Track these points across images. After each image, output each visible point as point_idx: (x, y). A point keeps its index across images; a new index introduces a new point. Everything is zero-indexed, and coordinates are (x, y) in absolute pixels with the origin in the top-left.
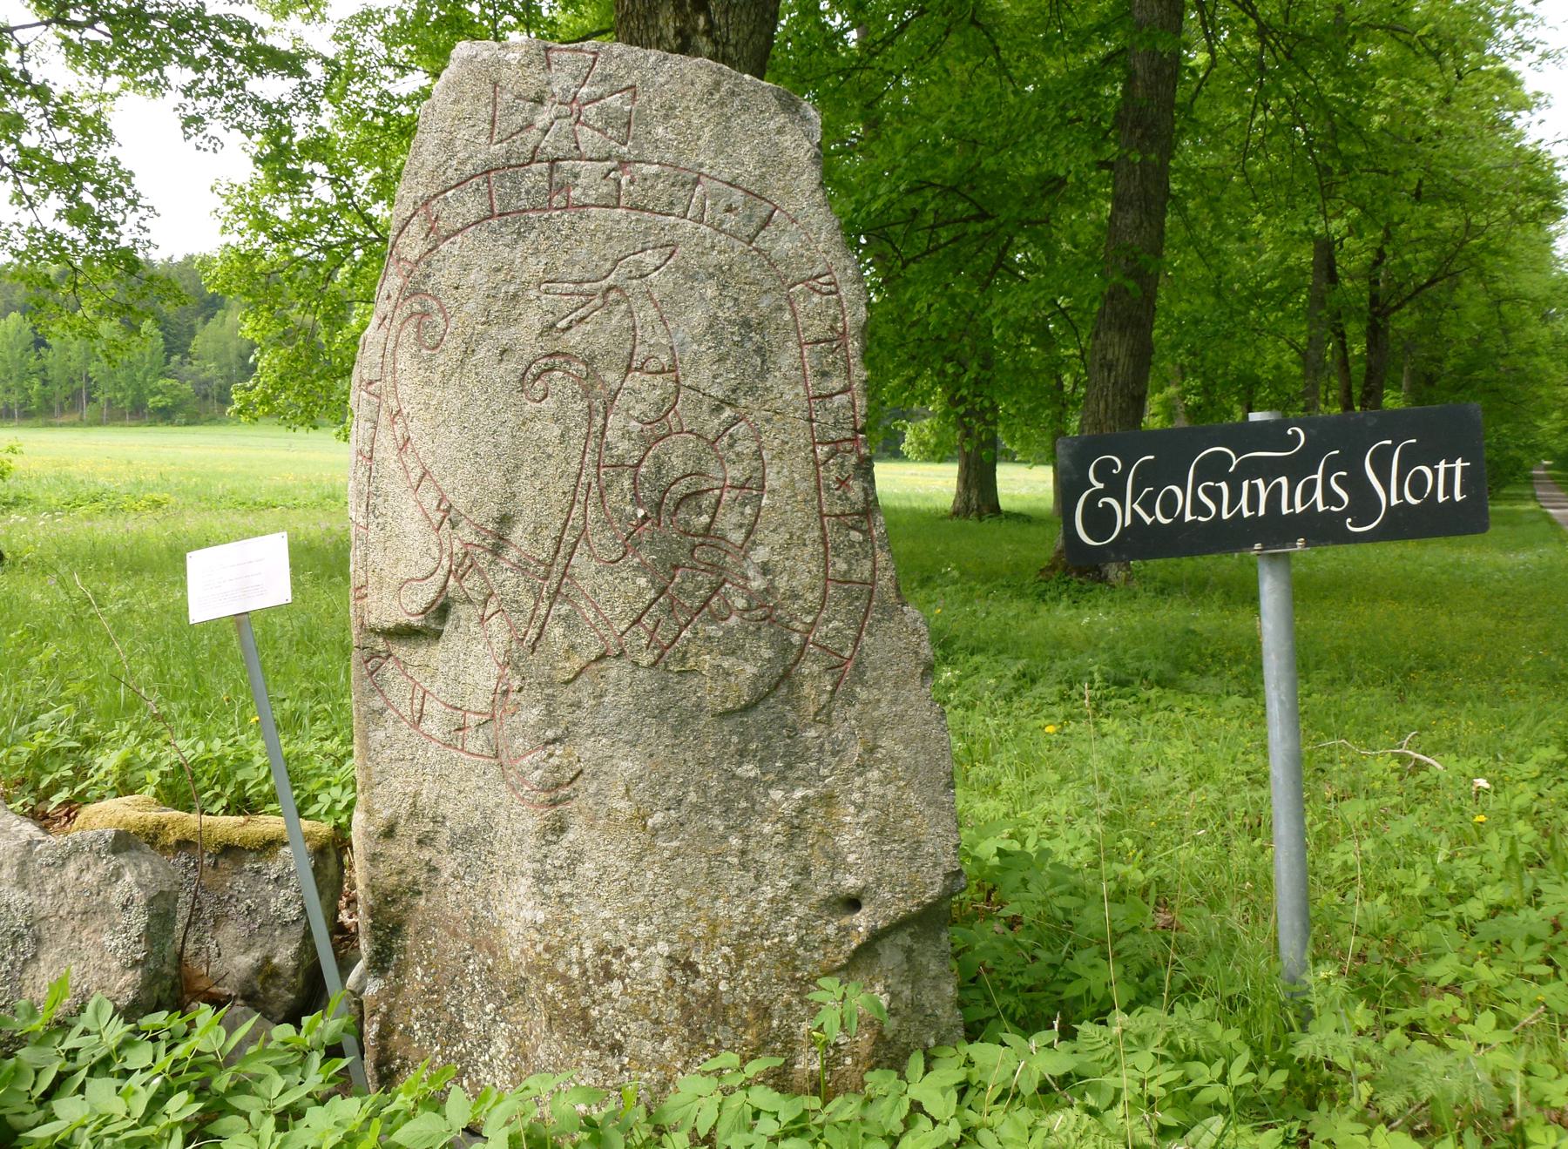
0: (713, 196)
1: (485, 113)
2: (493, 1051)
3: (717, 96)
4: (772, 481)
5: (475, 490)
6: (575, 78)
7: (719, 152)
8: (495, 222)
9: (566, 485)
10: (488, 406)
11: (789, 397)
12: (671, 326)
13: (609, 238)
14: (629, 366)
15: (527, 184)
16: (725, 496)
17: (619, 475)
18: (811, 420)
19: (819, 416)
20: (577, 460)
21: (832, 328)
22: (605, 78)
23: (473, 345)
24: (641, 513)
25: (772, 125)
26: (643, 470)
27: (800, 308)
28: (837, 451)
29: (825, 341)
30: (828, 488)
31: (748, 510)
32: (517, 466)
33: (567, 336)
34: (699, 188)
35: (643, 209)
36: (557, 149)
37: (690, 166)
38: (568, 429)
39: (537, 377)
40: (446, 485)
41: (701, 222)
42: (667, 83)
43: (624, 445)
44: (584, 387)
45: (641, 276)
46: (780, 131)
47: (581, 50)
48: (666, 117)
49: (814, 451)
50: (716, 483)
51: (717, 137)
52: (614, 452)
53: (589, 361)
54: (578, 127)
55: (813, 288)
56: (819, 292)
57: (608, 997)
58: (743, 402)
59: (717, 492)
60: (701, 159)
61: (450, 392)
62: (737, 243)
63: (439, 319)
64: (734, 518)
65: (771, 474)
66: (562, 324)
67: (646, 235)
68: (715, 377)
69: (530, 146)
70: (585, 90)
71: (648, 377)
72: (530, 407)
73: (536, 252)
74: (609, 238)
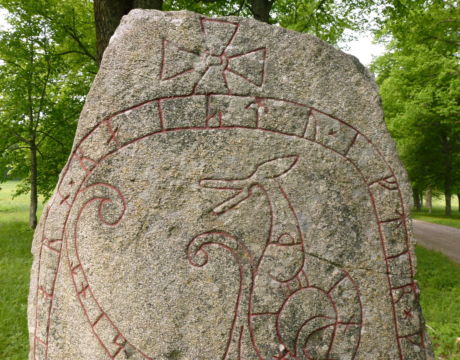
0: (321, 123)
1: (156, 58)
3: (320, 58)
4: (368, 317)
5: (149, 332)
6: (223, 39)
7: (323, 95)
8: (164, 135)
9: (224, 328)
10: (160, 269)
11: (374, 258)
12: (297, 211)
13: (252, 150)
14: (268, 240)
15: (189, 109)
16: (338, 330)
17: (265, 320)
18: (388, 273)
19: (392, 270)
20: (233, 310)
21: (397, 212)
22: (244, 41)
23: (147, 224)
24: (282, 348)
25: (353, 79)
26: (282, 316)
27: (377, 198)
28: (404, 293)
29: (393, 220)
30: (400, 318)
31: (353, 339)
32: (184, 315)
33: (221, 218)
34: (311, 118)
35: (275, 131)
36: (211, 86)
37: (305, 103)
38: (225, 286)
39: (199, 248)
40: (123, 325)
41: (314, 140)
42: (288, 47)
43: (268, 298)
44: (235, 255)
45: (275, 176)
46: (358, 84)
47: (226, 21)
48: (288, 69)
49: (391, 294)
50: (331, 321)
51: (322, 85)
52: (261, 304)
53: (239, 237)
54: (226, 72)
55: (384, 186)
56: (388, 188)
58: (346, 263)
59: (332, 327)
60: (312, 99)
61: (127, 257)
62: (338, 155)
63: (118, 203)
64: (345, 345)
65: (366, 312)
66: (218, 209)
67: (277, 148)
68: (328, 247)
69: (191, 83)
70: (230, 47)
71: (283, 248)
72: (193, 269)
73: (197, 158)
74: (252, 150)
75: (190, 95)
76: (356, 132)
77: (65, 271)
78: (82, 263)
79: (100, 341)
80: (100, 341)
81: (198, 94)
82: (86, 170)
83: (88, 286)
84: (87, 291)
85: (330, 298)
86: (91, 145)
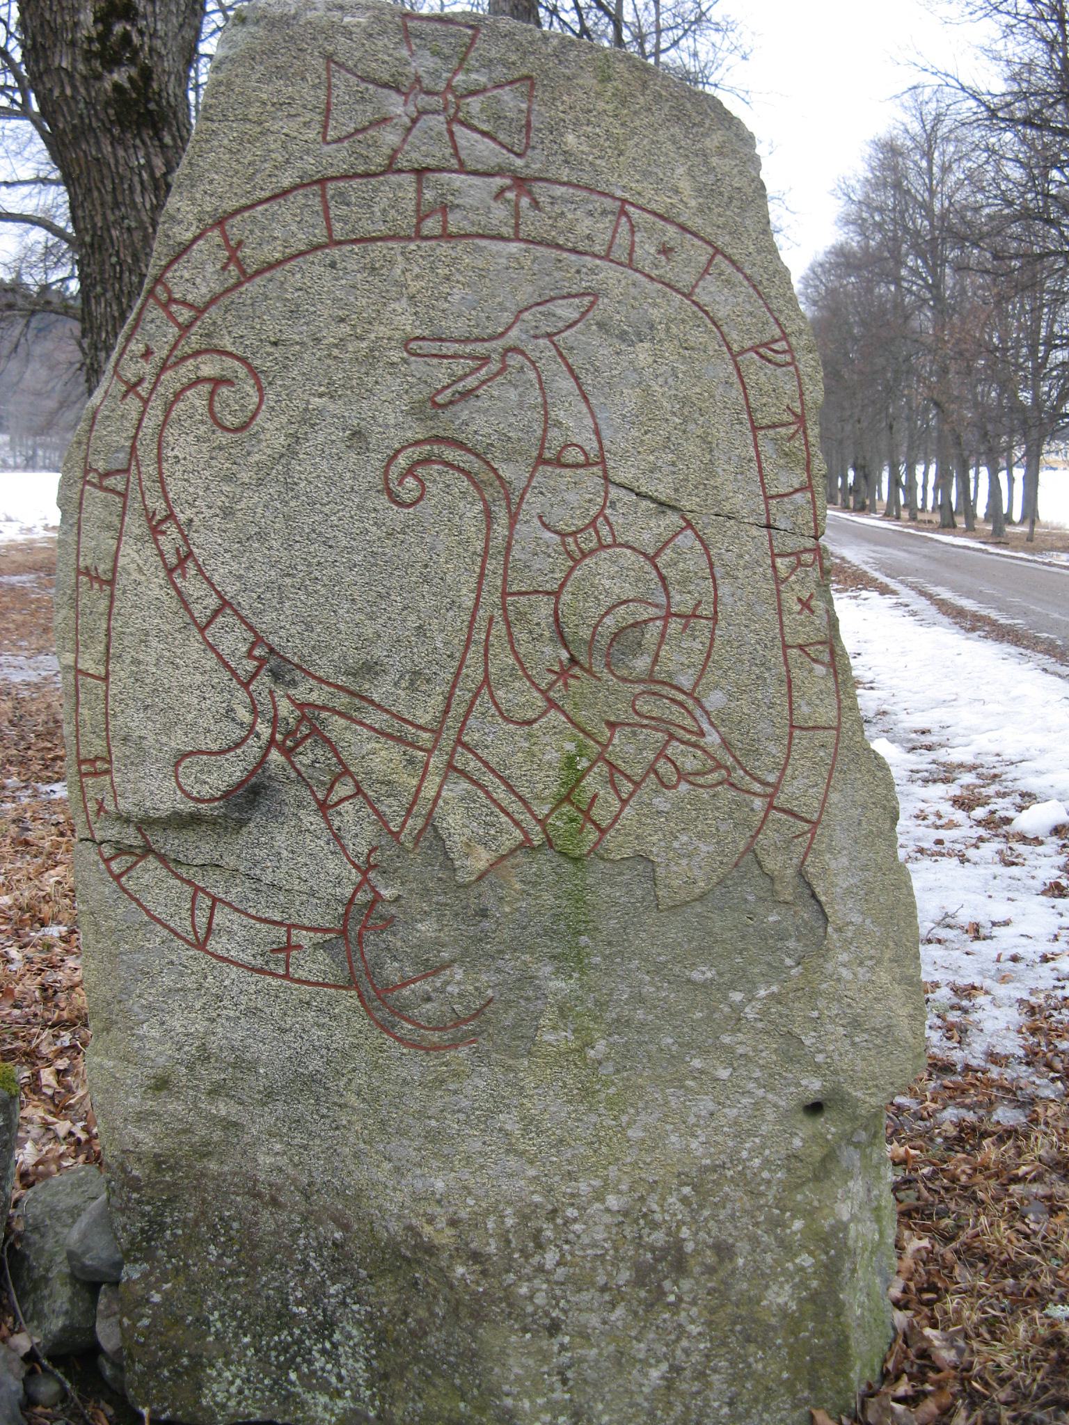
2: (337, 1336)
26: (566, 597)
40: (264, 622)
57: (540, 1269)
70: (460, 77)
75: (382, 173)
76: (711, 250)
77: (138, 531)
78: (177, 510)
79: (219, 656)
80: (219, 656)
81: (400, 171)
82: (179, 325)
83: (190, 554)
84: (190, 564)
85: (656, 567)
86: (187, 275)
